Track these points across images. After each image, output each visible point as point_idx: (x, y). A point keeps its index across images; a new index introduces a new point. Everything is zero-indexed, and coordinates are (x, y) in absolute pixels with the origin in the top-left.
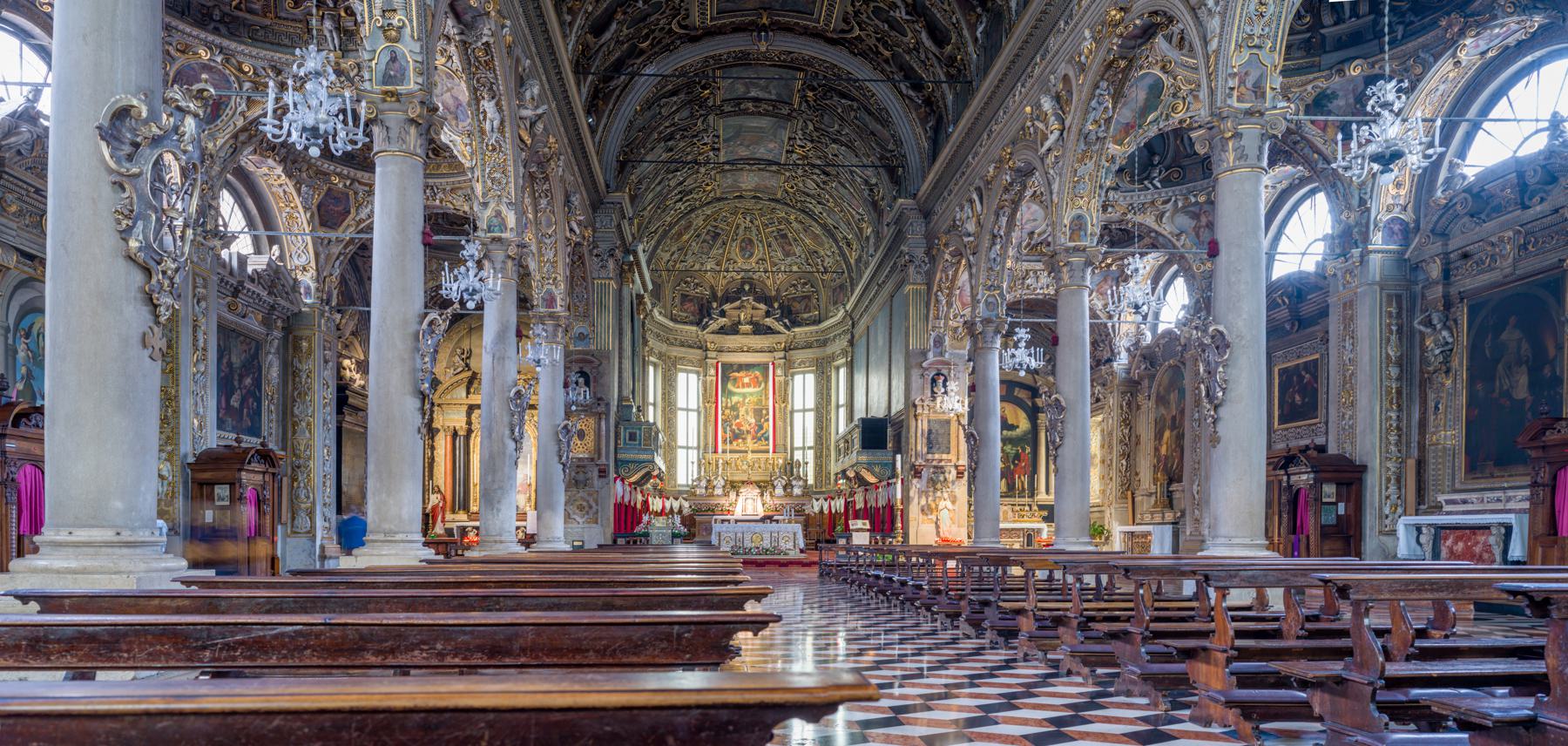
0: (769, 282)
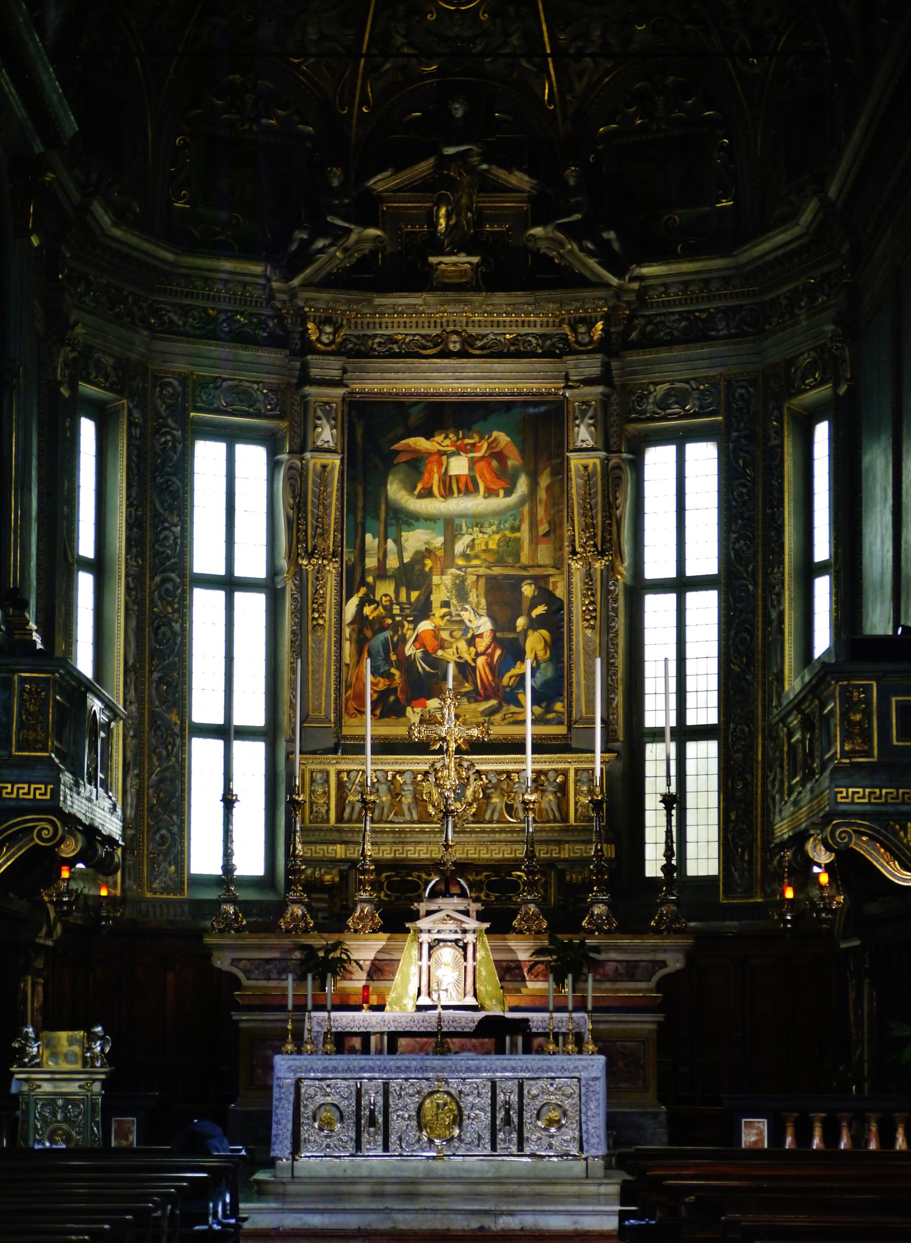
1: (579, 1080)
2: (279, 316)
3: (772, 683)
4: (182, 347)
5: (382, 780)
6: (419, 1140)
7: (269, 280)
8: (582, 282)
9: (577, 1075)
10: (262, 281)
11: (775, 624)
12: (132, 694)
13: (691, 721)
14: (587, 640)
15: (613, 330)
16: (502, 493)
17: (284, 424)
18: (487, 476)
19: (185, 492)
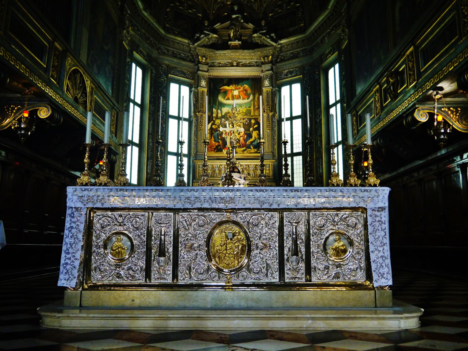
0: (255, 6)
1: (364, 210)
2: (192, 56)
3: (318, 138)
4: (166, 58)
5: (217, 167)
6: (209, 269)
7: (189, 44)
8: (266, 46)
9: (362, 205)
10: (188, 45)
11: (318, 123)
12: (151, 140)
13: (295, 151)
14: (268, 133)
15: (273, 59)
16: (246, 99)
17: (193, 81)
18: (243, 95)
19: (167, 93)
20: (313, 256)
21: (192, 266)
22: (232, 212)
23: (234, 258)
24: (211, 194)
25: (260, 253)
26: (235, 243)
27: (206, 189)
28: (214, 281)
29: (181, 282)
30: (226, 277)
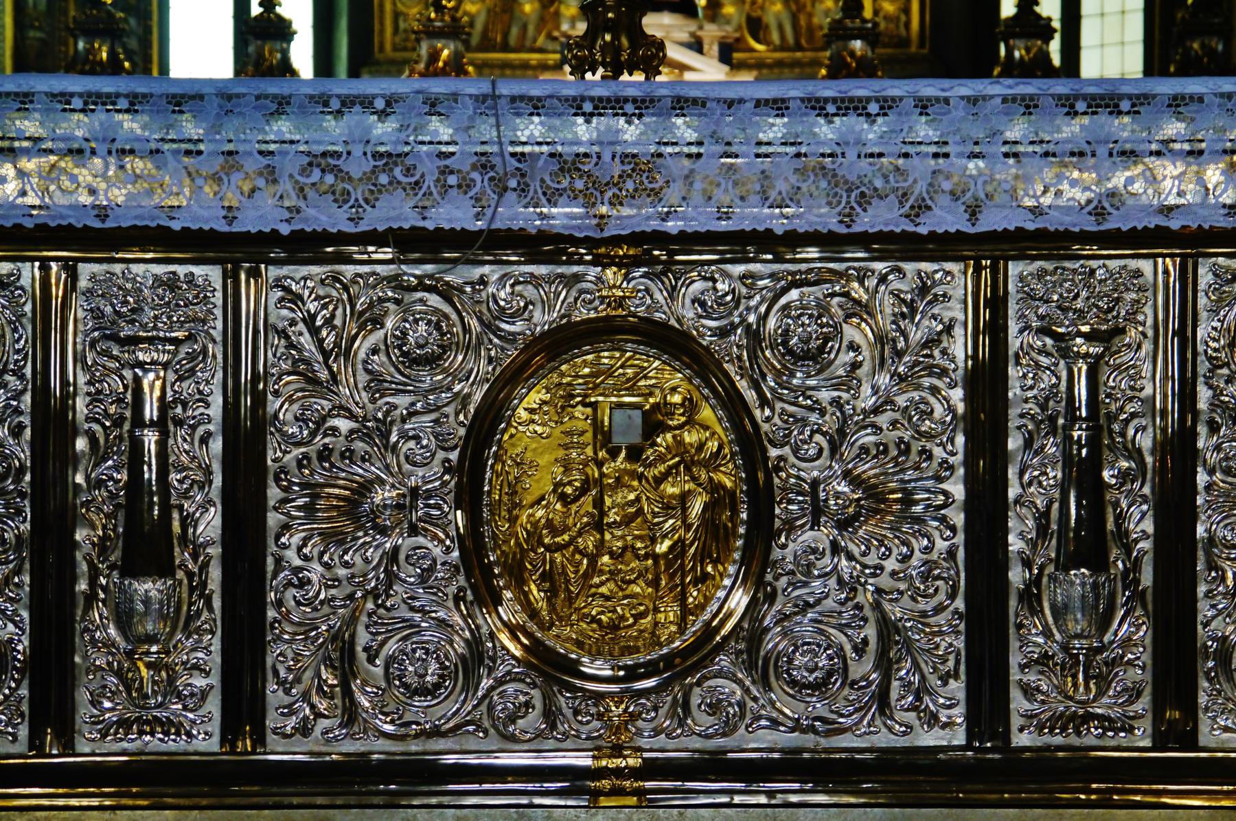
20: (1211, 566)
21: (363, 637)
22: (636, 262)
23: (655, 583)
24: (486, 130)
25: (836, 548)
26: (659, 480)
27: (455, 97)
28: (512, 738)
29: (279, 752)
30: (600, 716)
